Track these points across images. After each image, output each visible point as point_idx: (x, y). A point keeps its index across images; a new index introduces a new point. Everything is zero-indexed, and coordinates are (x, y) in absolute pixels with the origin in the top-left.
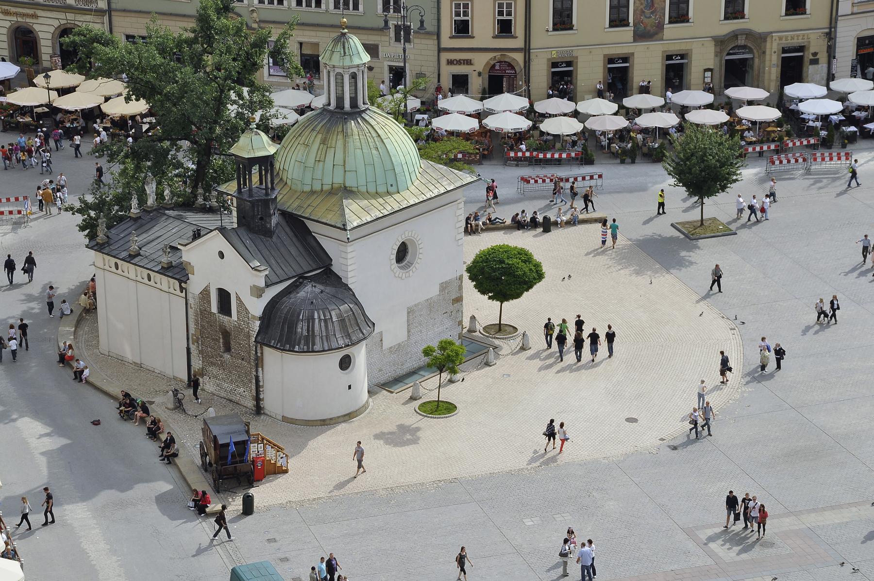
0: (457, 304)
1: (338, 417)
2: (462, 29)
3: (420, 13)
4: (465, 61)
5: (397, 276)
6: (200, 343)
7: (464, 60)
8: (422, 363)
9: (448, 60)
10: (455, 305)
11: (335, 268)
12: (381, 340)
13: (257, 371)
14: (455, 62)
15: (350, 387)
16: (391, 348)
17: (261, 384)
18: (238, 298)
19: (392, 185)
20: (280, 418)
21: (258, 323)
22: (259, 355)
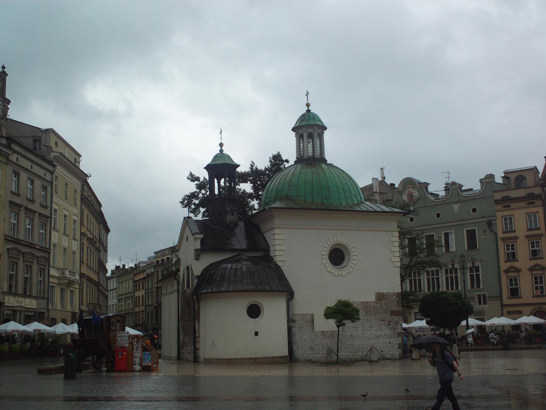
0: (395, 317)
1: (244, 359)
2: (514, 293)
3: (472, 258)
4: (518, 312)
5: (329, 271)
6: (182, 320)
7: (517, 311)
8: (359, 357)
9: (507, 311)
10: (393, 317)
11: (272, 254)
12: (313, 321)
13: (195, 324)
14: (512, 313)
15: (256, 334)
16: (324, 332)
17: (197, 334)
18: (191, 268)
19: (326, 199)
20: (203, 361)
21: (196, 280)
22: (196, 308)
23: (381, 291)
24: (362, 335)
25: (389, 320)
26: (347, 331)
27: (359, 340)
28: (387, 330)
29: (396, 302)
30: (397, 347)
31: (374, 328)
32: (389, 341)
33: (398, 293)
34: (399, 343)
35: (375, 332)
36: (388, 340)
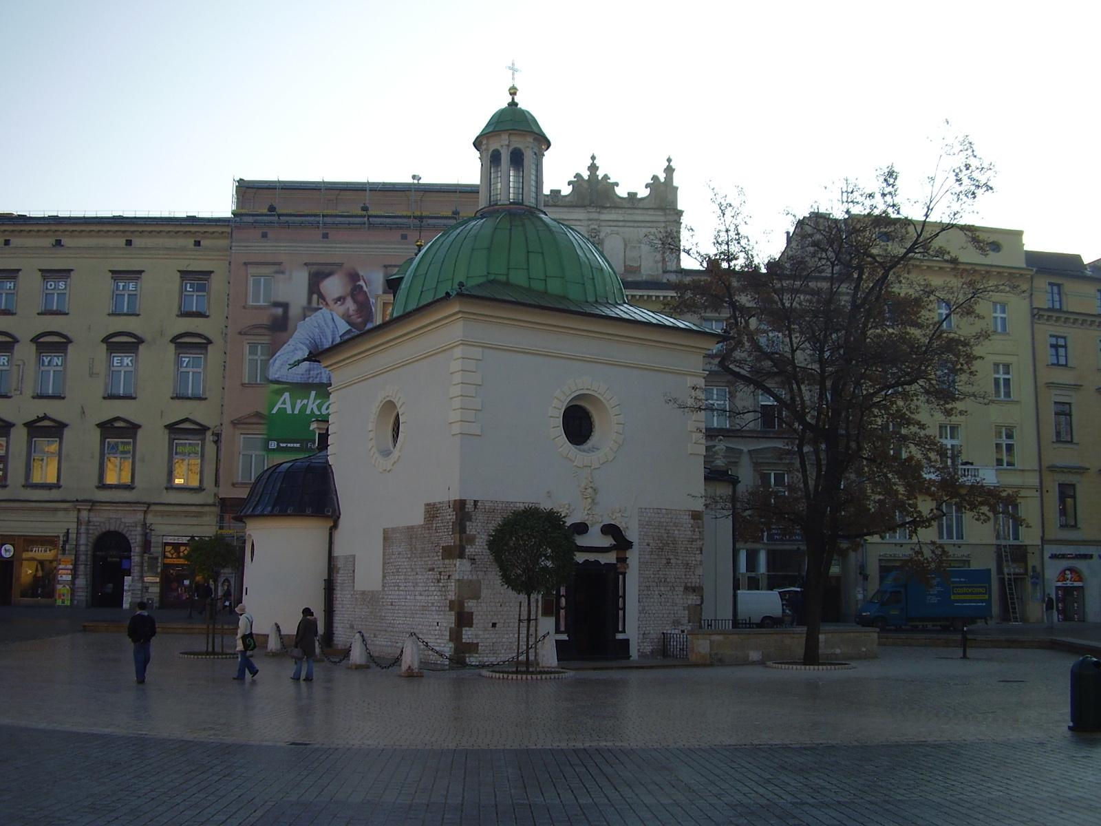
10: (447, 561)
12: (354, 571)
16: (363, 593)
23: (431, 501)
24: (403, 604)
25: (439, 570)
26: (387, 593)
27: (400, 615)
28: (435, 593)
29: (451, 524)
30: (448, 638)
31: (418, 589)
32: (438, 620)
33: (455, 501)
34: (450, 626)
35: (421, 598)
36: (437, 617)
